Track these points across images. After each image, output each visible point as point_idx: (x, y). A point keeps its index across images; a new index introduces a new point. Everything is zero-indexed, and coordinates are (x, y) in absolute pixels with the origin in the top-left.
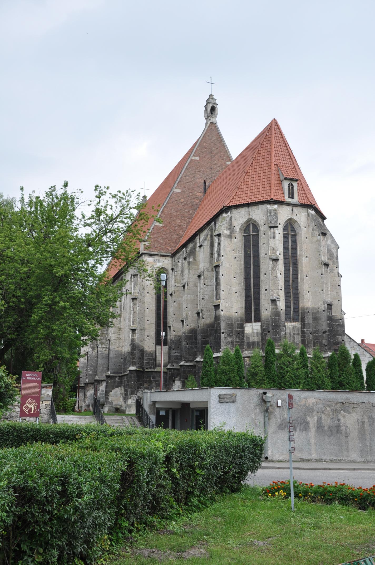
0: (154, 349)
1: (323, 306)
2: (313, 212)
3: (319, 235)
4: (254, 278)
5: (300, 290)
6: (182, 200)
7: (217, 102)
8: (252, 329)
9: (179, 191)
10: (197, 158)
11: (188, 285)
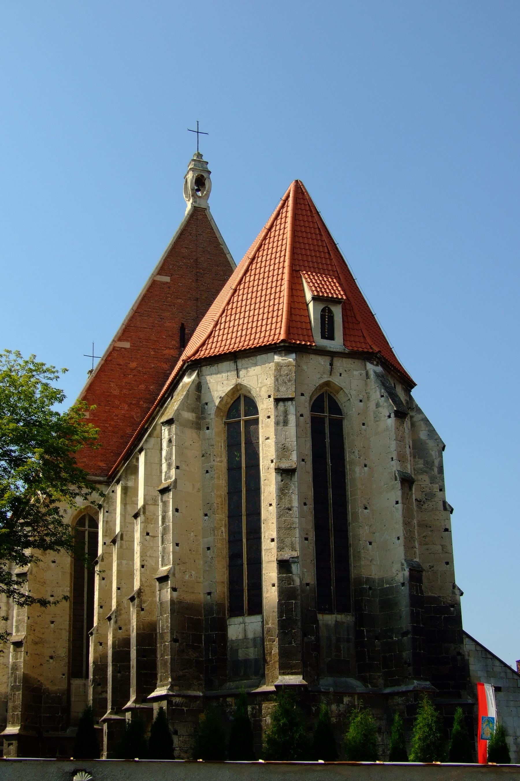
0: (65, 687)
1: (400, 575)
2: (379, 369)
3: (389, 417)
4: (247, 515)
5: (351, 541)
6: (133, 365)
7: (210, 167)
11: (122, 539)
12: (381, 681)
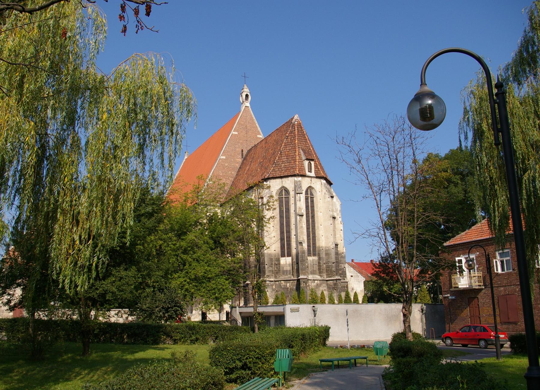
2: (325, 181)
5: (316, 235)
6: (226, 164)
8: (286, 261)
9: (224, 157)
10: (236, 133)
12: (325, 276)
